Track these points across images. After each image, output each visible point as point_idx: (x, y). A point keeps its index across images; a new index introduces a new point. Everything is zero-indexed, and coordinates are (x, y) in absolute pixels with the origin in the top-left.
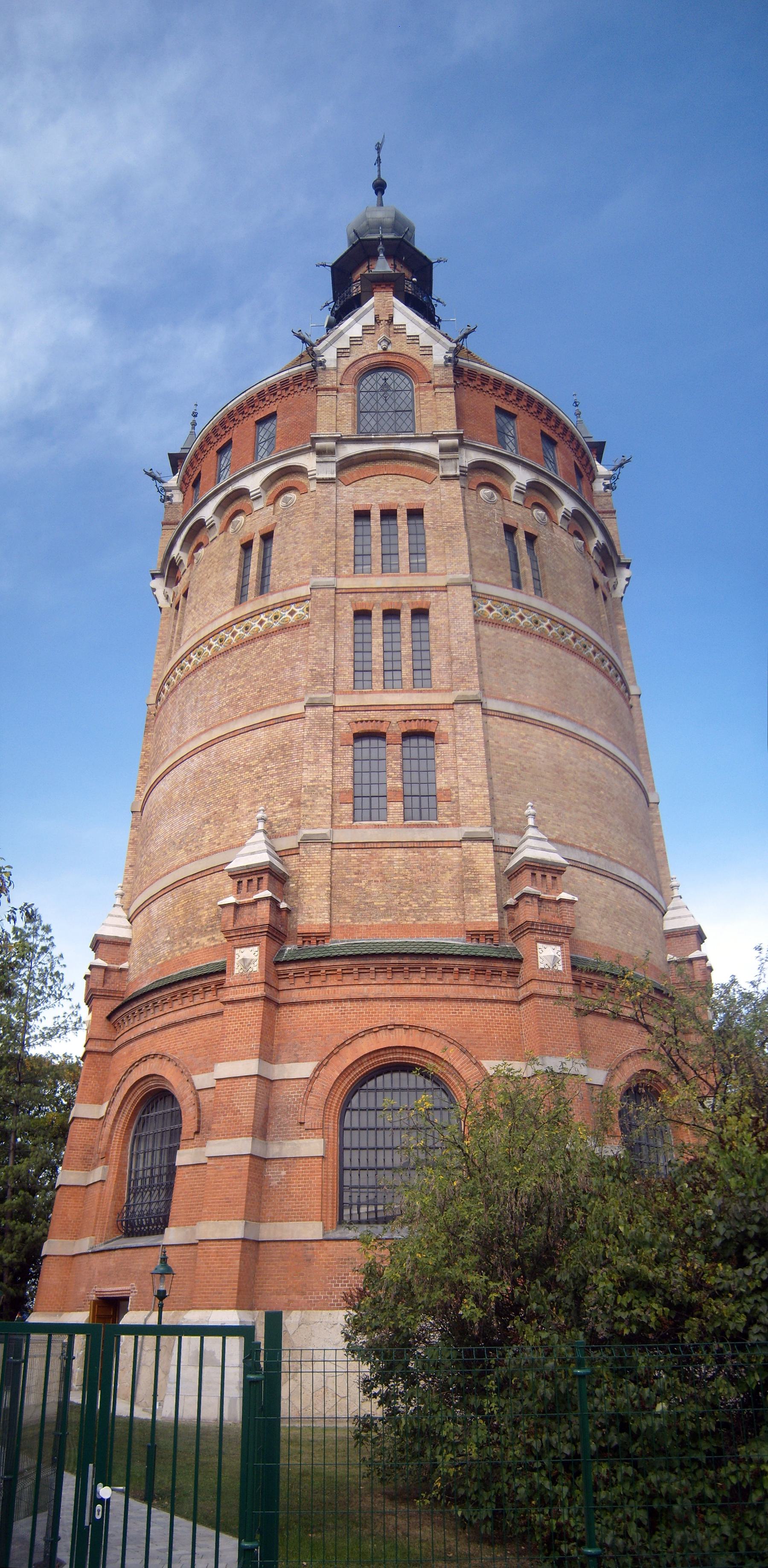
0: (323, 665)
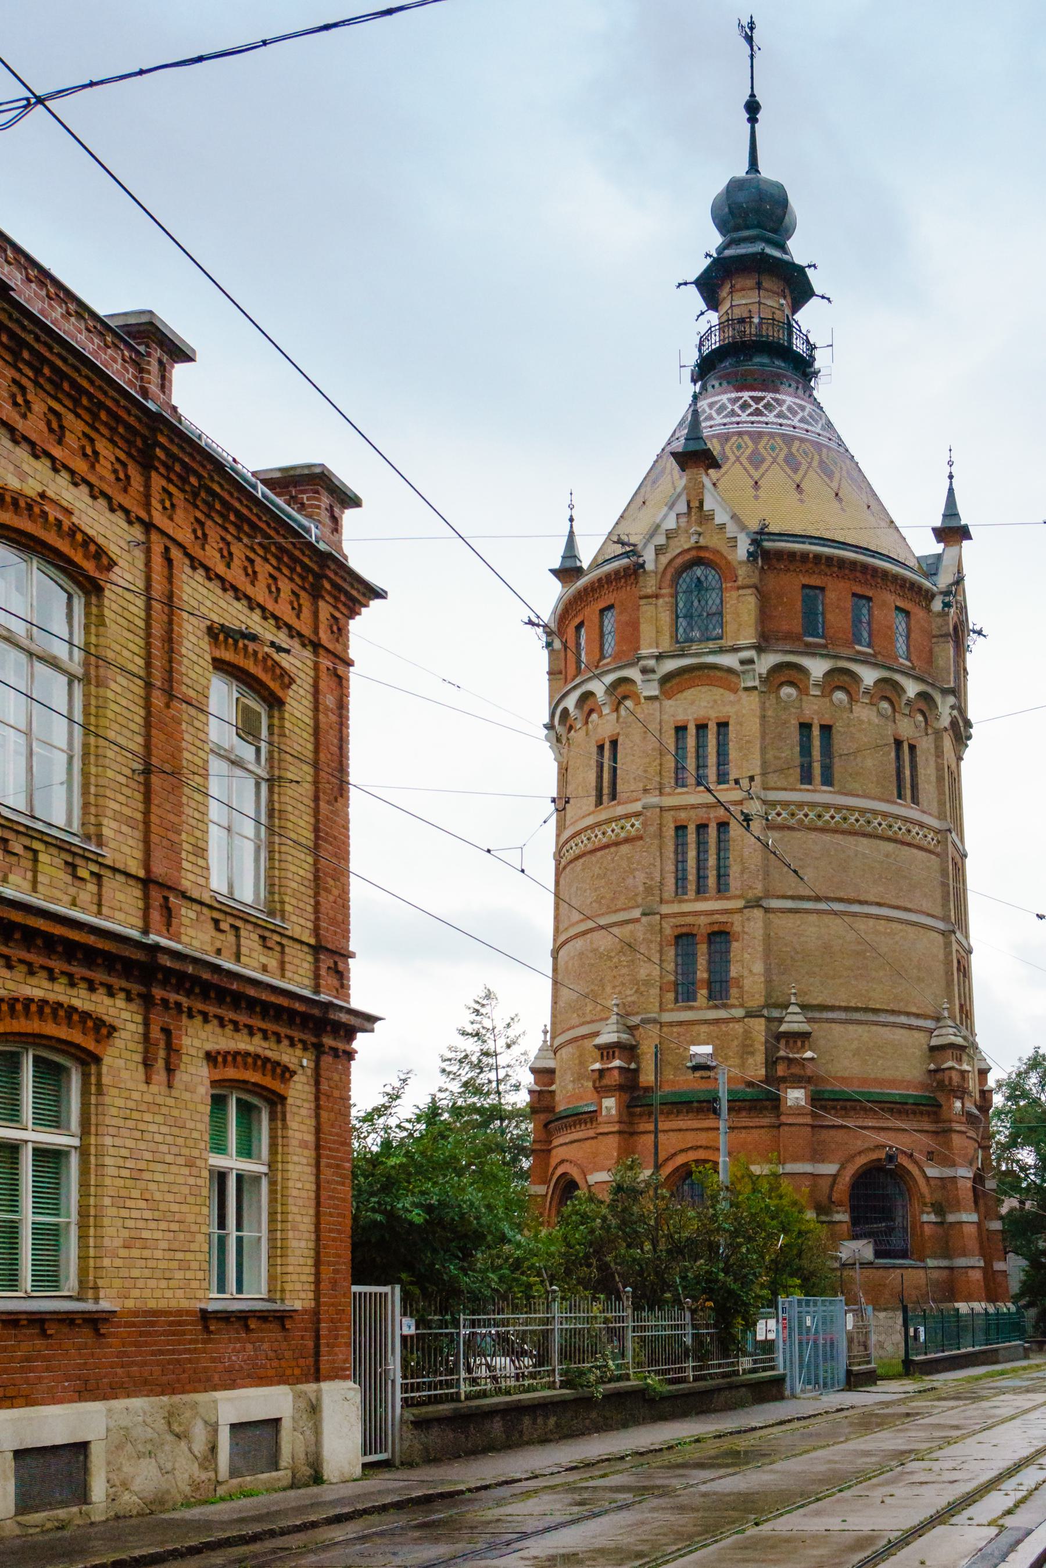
0: (652, 879)
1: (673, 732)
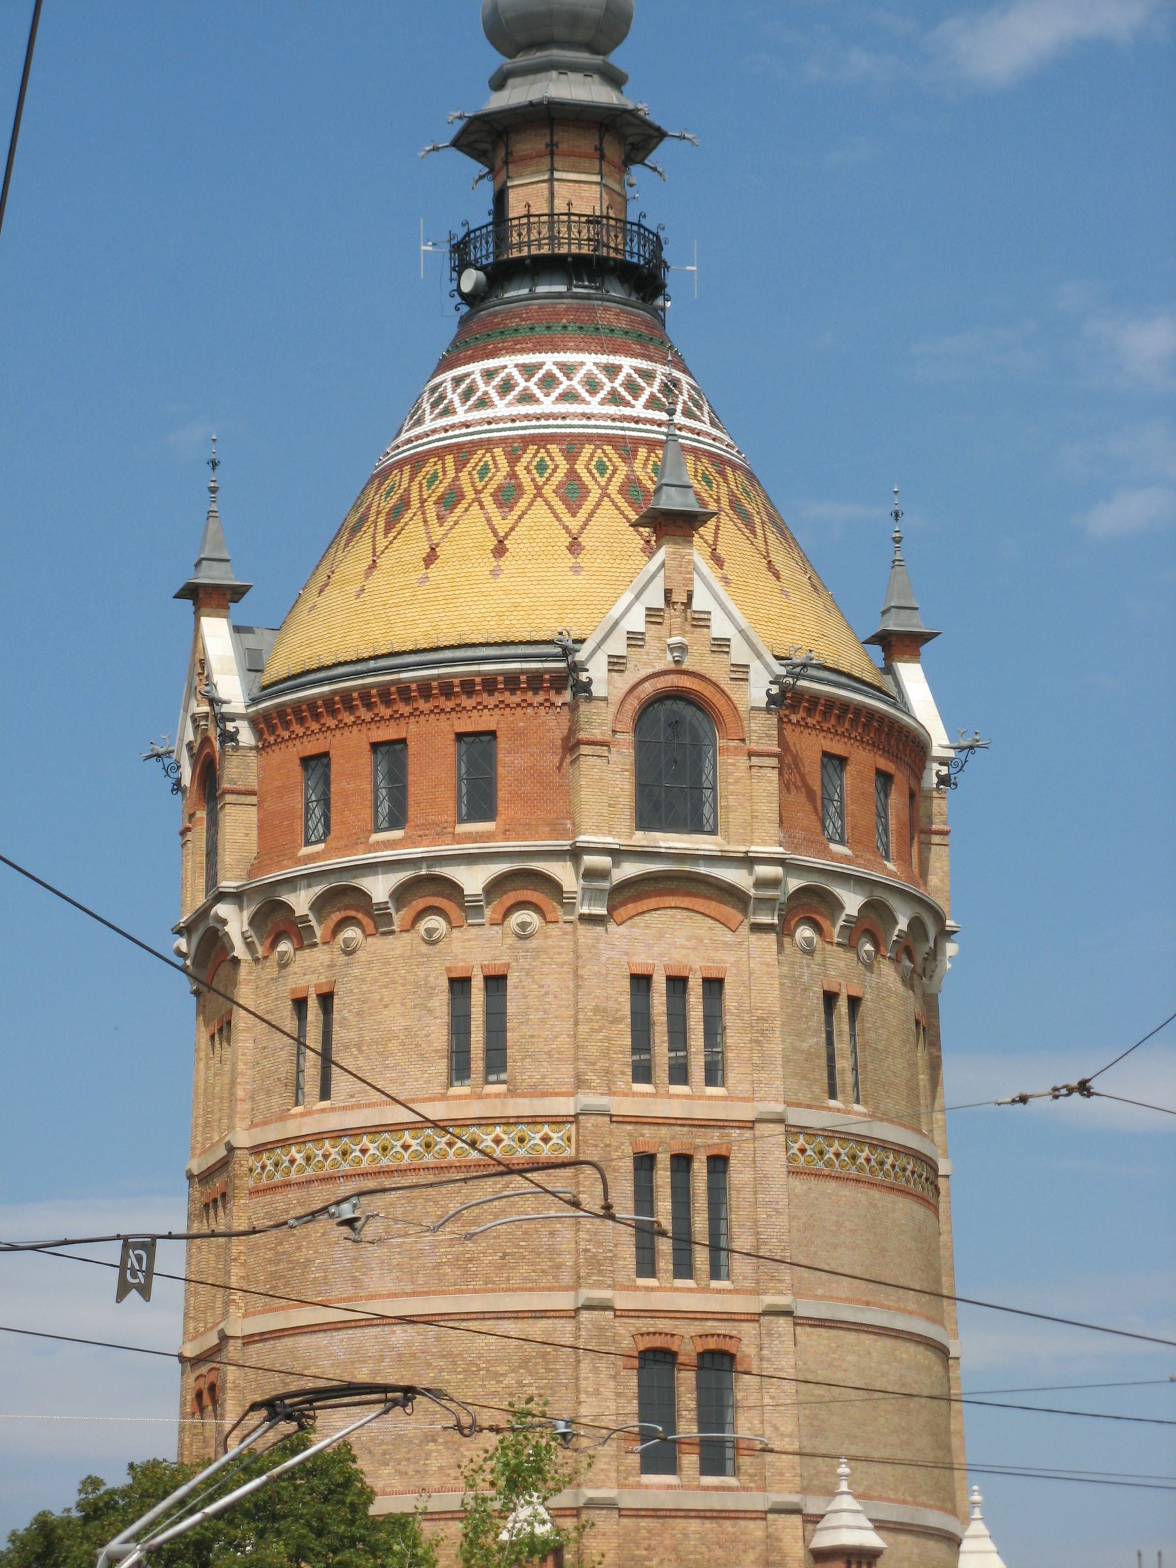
1: (626, 984)
